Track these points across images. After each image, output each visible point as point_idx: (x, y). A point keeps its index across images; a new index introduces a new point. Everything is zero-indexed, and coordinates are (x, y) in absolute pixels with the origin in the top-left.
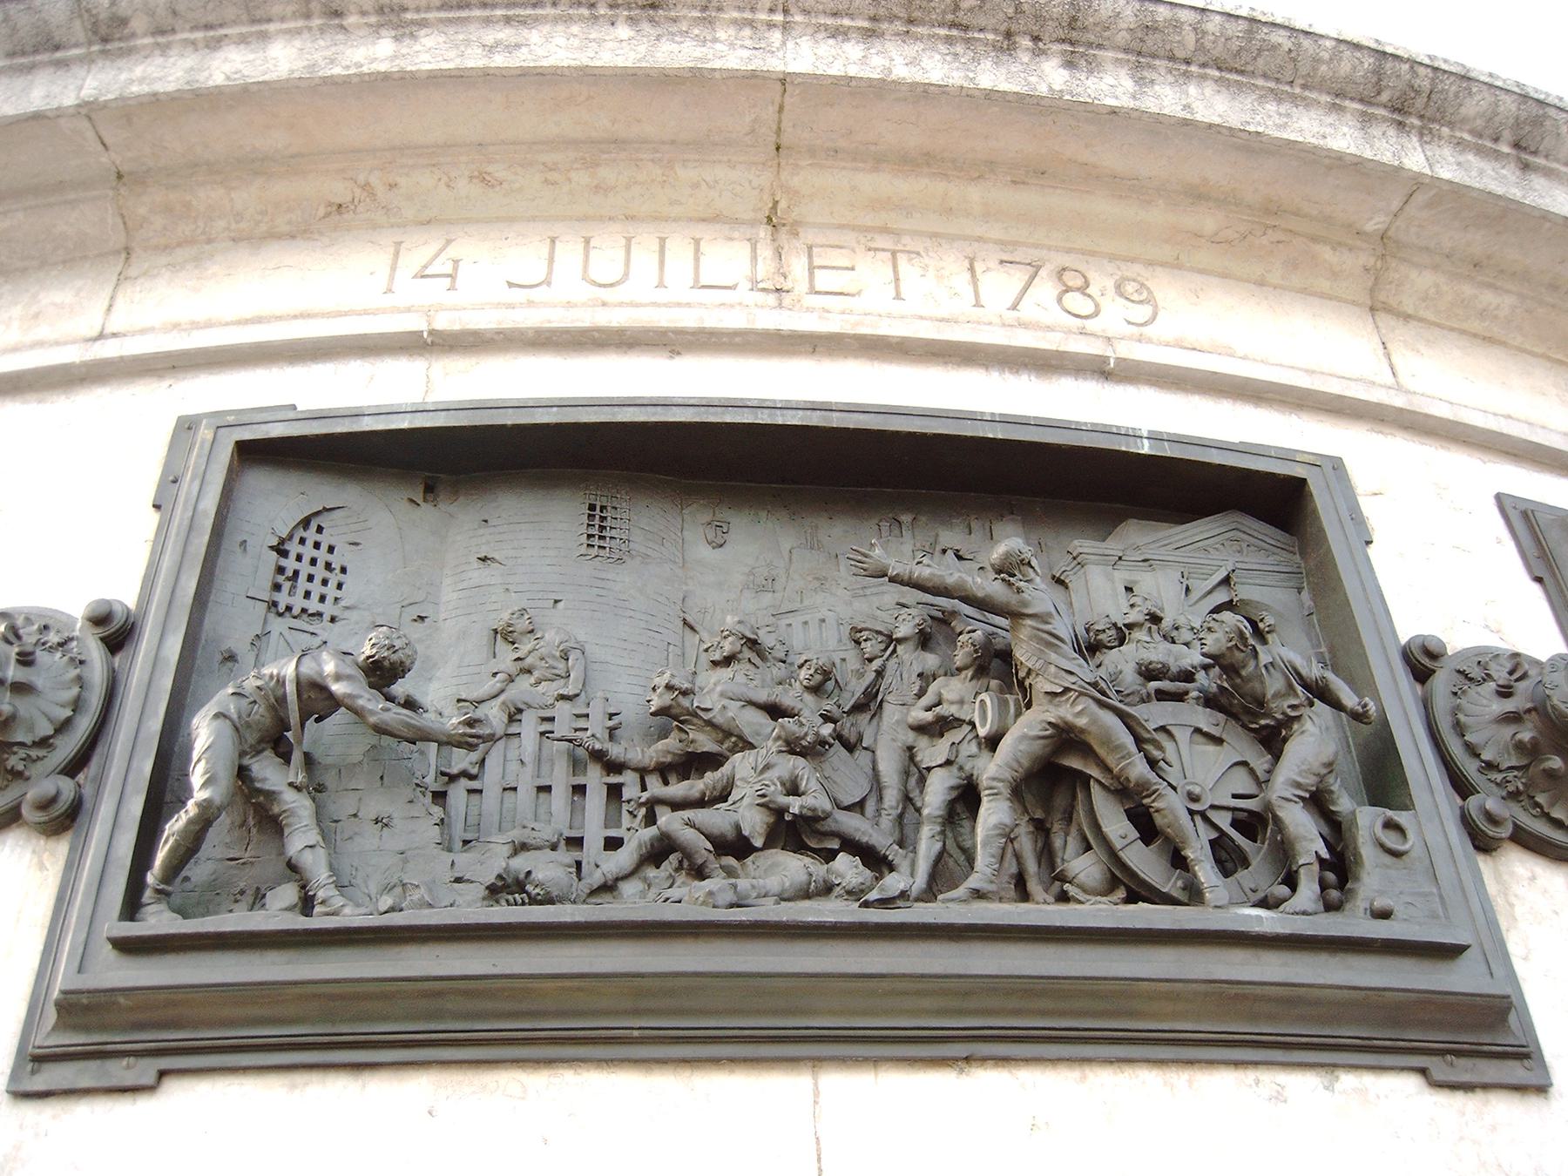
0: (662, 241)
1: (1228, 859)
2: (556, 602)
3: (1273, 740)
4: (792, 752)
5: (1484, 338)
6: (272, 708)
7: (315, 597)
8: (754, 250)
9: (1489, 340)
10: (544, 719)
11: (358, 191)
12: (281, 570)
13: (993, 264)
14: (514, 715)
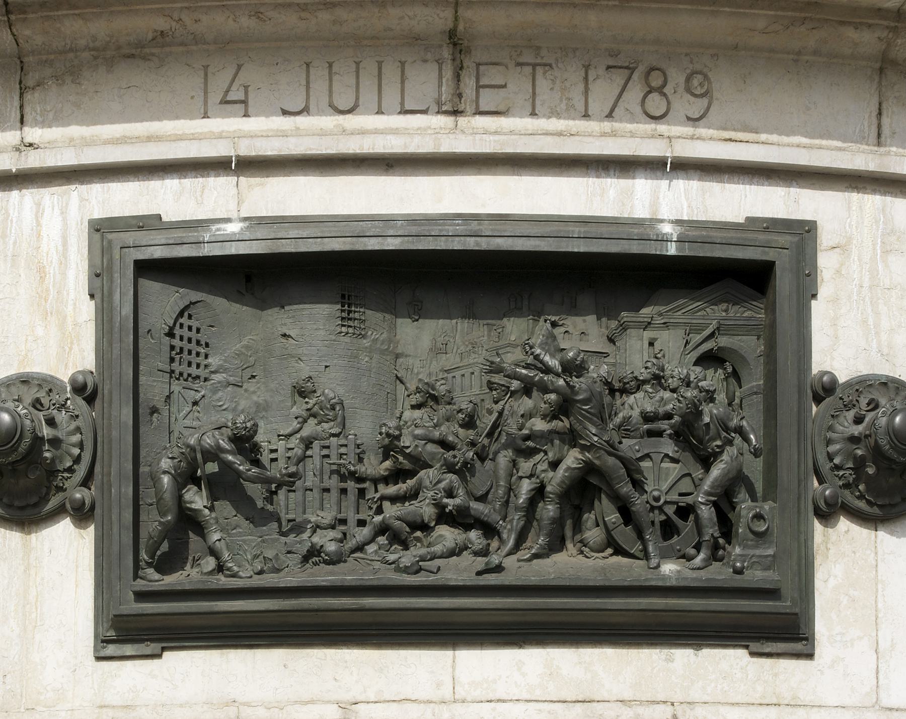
0: (380, 64)
1: (668, 530)
2: (326, 367)
3: (706, 462)
4: (450, 472)
6: (188, 463)
7: (194, 366)
8: (440, 70)
10: (324, 447)
11: (174, 24)
12: (172, 348)
13: (601, 71)
14: (308, 443)
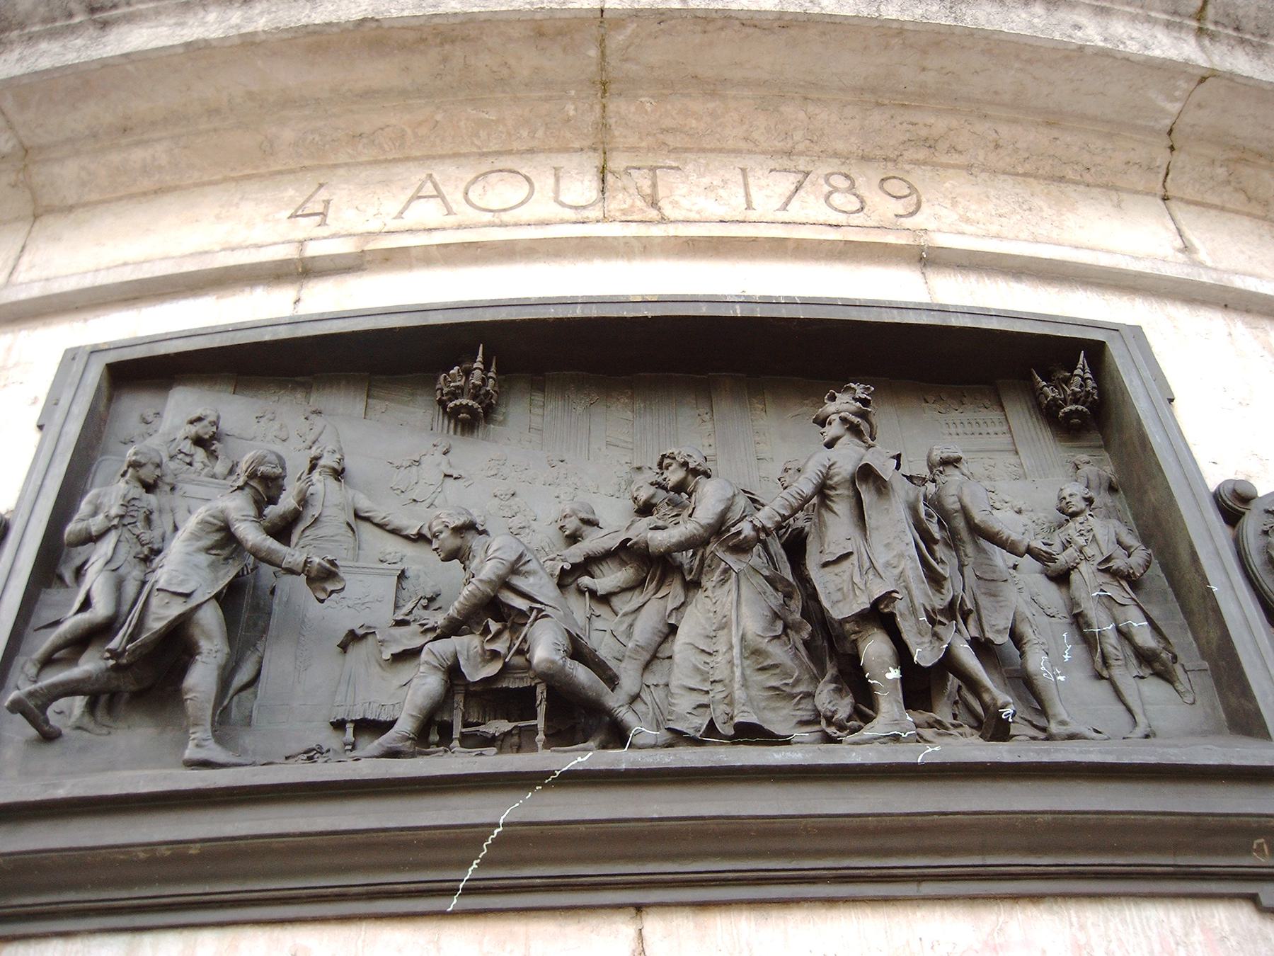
5: (156, 192)
9: (160, 191)
